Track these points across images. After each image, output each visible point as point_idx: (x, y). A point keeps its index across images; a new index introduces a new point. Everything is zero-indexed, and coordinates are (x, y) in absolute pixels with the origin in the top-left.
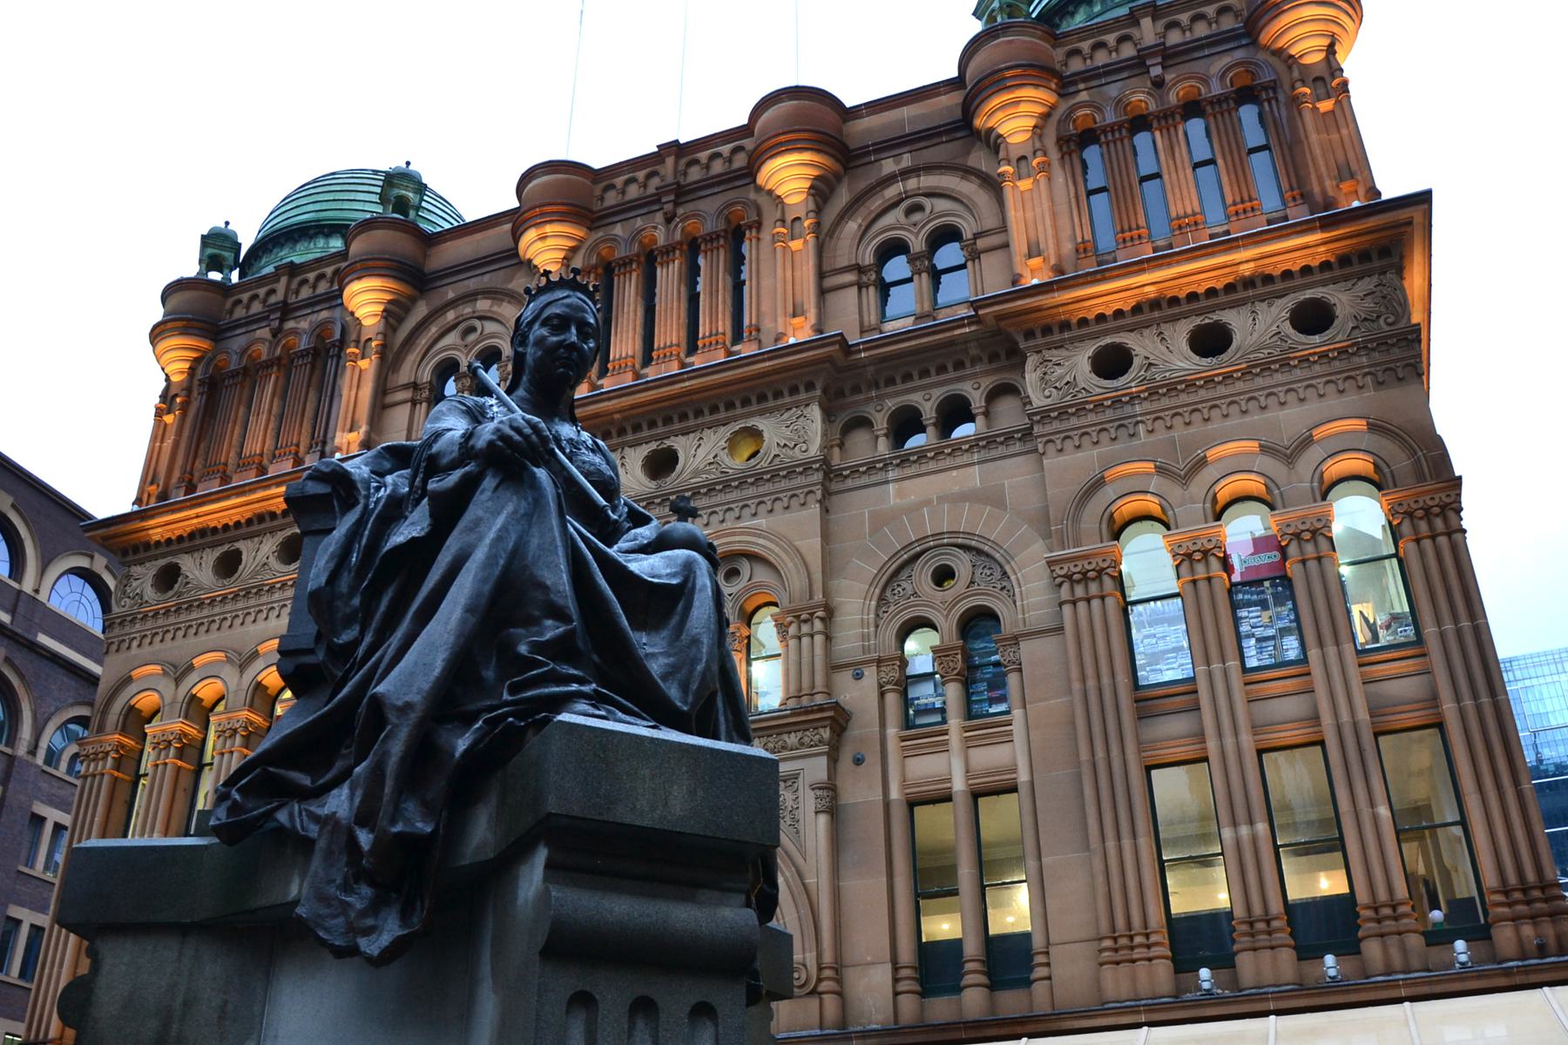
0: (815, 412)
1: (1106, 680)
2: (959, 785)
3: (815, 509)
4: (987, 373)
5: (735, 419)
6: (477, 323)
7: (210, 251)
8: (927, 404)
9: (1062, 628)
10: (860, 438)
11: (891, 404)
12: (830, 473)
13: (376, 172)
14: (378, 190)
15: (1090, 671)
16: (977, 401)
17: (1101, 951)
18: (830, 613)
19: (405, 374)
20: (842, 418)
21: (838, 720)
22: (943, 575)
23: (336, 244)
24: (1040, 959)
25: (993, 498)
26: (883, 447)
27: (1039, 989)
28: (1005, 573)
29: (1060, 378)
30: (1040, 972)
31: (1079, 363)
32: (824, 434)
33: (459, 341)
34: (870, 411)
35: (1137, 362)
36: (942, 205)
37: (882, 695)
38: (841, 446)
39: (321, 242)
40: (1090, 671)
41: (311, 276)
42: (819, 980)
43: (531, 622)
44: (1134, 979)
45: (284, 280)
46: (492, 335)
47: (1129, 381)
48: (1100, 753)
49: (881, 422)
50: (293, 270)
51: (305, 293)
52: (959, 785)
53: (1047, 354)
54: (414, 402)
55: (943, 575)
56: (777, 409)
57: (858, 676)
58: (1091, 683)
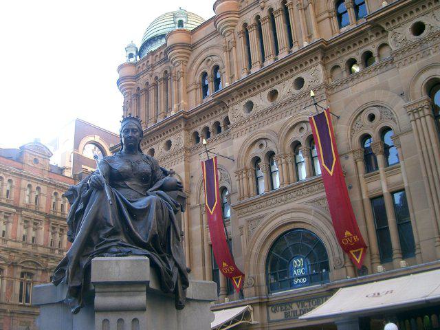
0: (320, 67)
1: (429, 147)
2: (385, 191)
4: (376, 41)
6: (210, 58)
7: (129, 53)
8: (357, 55)
9: (412, 130)
10: (337, 72)
12: (328, 87)
13: (169, 13)
15: (423, 144)
16: (374, 51)
17: (436, 242)
19: (191, 81)
20: (330, 67)
22: (372, 117)
23: (164, 41)
24: (417, 247)
25: (385, 87)
26: (345, 75)
27: (418, 257)
28: (392, 113)
29: (401, 38)
30: (417, 252)
31: (406, 31)
33: (206, 66)
34: (338, 63)
35: (427, 27)
37: (356, 163)
38: (331, 77)
39: (159, 41)
40: (423, 144)
41: (158, 54)
42: (345, 263)
43: (104, 228)
45: (151, 57)
46: (216, 61)
48: (429, 173)
49: (343, 65)
50: (152, 53)
51: (158, 60)
52: (385, 191)
53: (395, 30)
54: (196, 89)
55: (372, 117)
56: (307, 69)
57: (347, 158)
58: (424, 149)
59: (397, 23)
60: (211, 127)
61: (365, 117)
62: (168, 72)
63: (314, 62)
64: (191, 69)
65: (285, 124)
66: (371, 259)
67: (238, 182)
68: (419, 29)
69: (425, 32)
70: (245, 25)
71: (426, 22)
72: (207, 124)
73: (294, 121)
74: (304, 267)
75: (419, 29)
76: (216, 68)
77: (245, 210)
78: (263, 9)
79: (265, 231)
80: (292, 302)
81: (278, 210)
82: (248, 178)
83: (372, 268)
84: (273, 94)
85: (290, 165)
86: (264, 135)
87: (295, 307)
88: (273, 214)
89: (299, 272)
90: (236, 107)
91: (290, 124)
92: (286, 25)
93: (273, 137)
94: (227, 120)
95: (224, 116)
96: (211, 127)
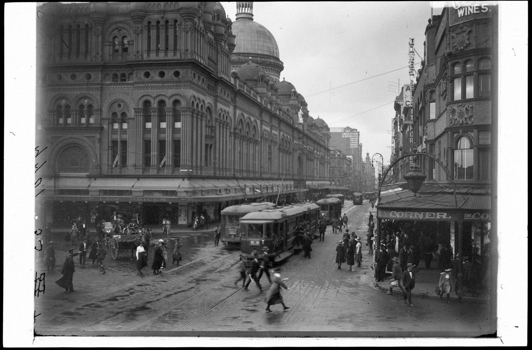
0: (100, 73)
2: (119, 140)
3: (99, 92)
11: (113, 72)
18: (101, 110)
21: (102, 128)
31: (142, 74)
32: (102, 77)
36: (125, 31)
61: (116, 105)
66: (108, 167)
68: (147, 75)
69: (149, 78)
71: (151, 74)
75: (147, 75)
78: (74, 22)
81: (69, 136)
85: (78, 115)
91: (80, 96)
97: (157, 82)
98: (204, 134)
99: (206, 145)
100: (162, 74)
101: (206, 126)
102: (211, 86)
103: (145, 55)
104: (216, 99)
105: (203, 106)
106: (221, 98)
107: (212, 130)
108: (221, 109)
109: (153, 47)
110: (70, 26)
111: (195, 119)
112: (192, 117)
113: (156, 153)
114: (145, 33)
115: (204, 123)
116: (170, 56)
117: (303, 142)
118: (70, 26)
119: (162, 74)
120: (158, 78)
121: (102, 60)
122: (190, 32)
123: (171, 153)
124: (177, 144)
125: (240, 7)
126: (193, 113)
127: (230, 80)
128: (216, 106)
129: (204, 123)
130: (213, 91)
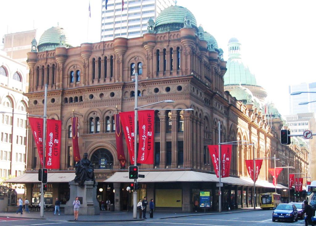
0: (121, 91)
5: (111, 90)
14: (59, 37)
16: (141, 91)
31: (152, 89)
34: (128, 91)
44: (150, 166)
47: (157, 93)
49: (129, 92)
59: (150, 85)
60: (73, 98)
62: (55, 65)
63: (119, 89)
64: (66, 67)
65: (105, 109)
67: (83, 126)
68: (157, 90)
70: (94, 59)
72: (72, 96)
73: (109, 109)
74: (105, 162)
75: (157, 90)
76: (78, 71)
77: (85, 138)
79: (92, 147)
80: (99, 174)
81: (98, 140)
82: (87, 125)
83: (127, 167)
84: (102, 95)
86: (96, 110)
87: (100, 175)
88: (97, 141)
89: (103, 163)
90: (86, 95)
91: (107, 110)
92: (111, 66)
93: (100, 112)
94: (81, 98)
95: (80, 95)
96: (73, 98)
97: (164, 95)
98: (202, 137)
99: (205, 147)
100: (168, 89)
101: (205, 132)
102: (208, 100)
103: (155, 76)
104: (212, 109)
105: (201, 114)
106: (216, 110)
107: (209, 135)
108: (216, 119)
109: (161, 68)
110: (100, 58)
111: (195, 124)
112: (193, 122)
113: (164, 152)
114: (155, 58)
115: (202, 128)
116: (175, 75)
117: (286, 154)
118: (100, 58)
119: (168, 89)
120: (164, 92)
121: (123, 80)
122: (189, 56)
123: (176, 151)
124: (180, 144)
125: (231, 49)
126: (193, 119)
127: (223, 96)
128: (212, 116)
129: (202, 128)
130: (209, 104)
